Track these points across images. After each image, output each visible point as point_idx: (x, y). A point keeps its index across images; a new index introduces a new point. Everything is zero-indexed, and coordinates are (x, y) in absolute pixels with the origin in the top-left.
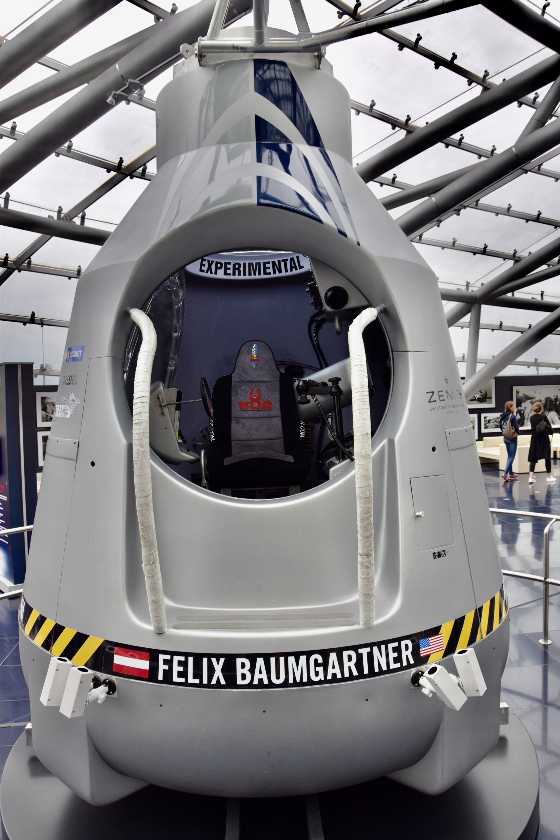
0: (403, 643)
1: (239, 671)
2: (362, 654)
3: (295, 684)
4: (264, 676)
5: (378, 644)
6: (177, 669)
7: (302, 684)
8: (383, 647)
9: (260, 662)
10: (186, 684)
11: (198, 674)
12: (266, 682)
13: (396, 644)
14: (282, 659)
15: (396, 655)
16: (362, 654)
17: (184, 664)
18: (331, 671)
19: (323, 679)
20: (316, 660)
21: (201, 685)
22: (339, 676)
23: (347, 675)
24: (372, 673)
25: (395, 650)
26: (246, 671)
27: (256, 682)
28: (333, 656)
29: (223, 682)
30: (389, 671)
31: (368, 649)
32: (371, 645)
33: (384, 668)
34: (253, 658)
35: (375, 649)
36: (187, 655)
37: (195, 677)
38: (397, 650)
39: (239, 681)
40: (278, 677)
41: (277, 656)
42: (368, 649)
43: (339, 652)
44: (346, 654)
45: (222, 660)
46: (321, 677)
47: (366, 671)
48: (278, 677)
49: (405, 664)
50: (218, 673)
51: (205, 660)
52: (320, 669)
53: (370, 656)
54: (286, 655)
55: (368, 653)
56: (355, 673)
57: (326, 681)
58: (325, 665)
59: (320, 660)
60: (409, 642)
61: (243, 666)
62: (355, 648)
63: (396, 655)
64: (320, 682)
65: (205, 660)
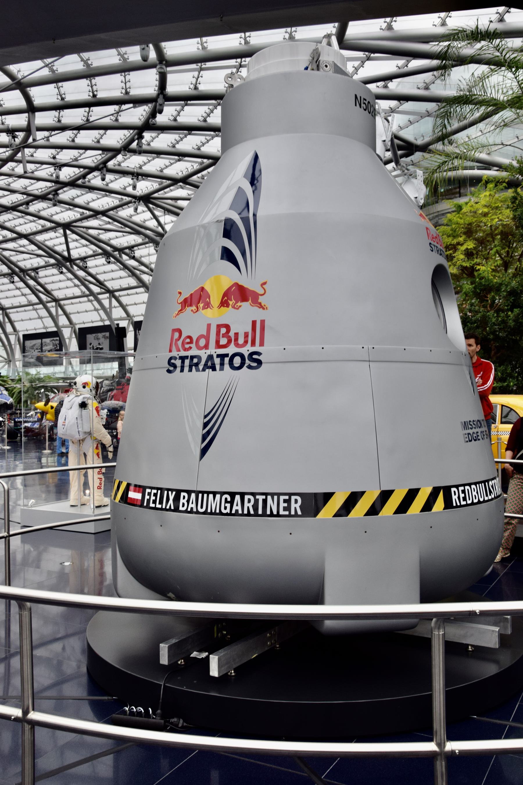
0: (293, 498)
1: (182, 501)
2: (258, 499)
3: (211, 513)
4: (194, 506)
5: (272, 495)
6: (153, 498)
7: (215, 514)
8: (276, 497)
9: (193, 496)
10: (155, 508)
11: (161, 502)
12: (195, 510)
13: (287, 497)
14: (205, 495)
15: (286, 505)
16: (258, 499)
17: (155, 495)
18: (235, 508)
19: (229, 512)
20: (226, 499)
21: (161, 509)
22: (240, 512)
23: (246, 512)
24: (264, 515)
25: (285, 501)
26: (185, 501)
27: (189, 510)
28: (238, 498)
29: (172, 508)
30: (278, 515)
31: (264, 497)
32: (266, 494)
33: (275, 512)
34: (189, 492)
35: (269, 498)
36: (158, 489)
37: (159, 504)
38: (288, 501)
39: (181, 508)
40: (202, 507)
41: (203, 493)
42: (264, 497)
43: (243, 495)
44: (247, 497)
45: (174, 493)
46: (228, 511)
47: (260, 512)
48: (202, 507)
49: (293, 513)
50: (171, 502)
51: (166, 492)
52: (228, 505)
53: (265, 501)
54: (208, 493)
55: (263, 500)
56: (252, 512)
57: (230, 514)
58: (232, 503)
59: (229, 499)
60: (299, 499)
61: (184, 497)
62: (253, 494)
63: (286, 505)
64: (227, 514)
65: (166, 492)
